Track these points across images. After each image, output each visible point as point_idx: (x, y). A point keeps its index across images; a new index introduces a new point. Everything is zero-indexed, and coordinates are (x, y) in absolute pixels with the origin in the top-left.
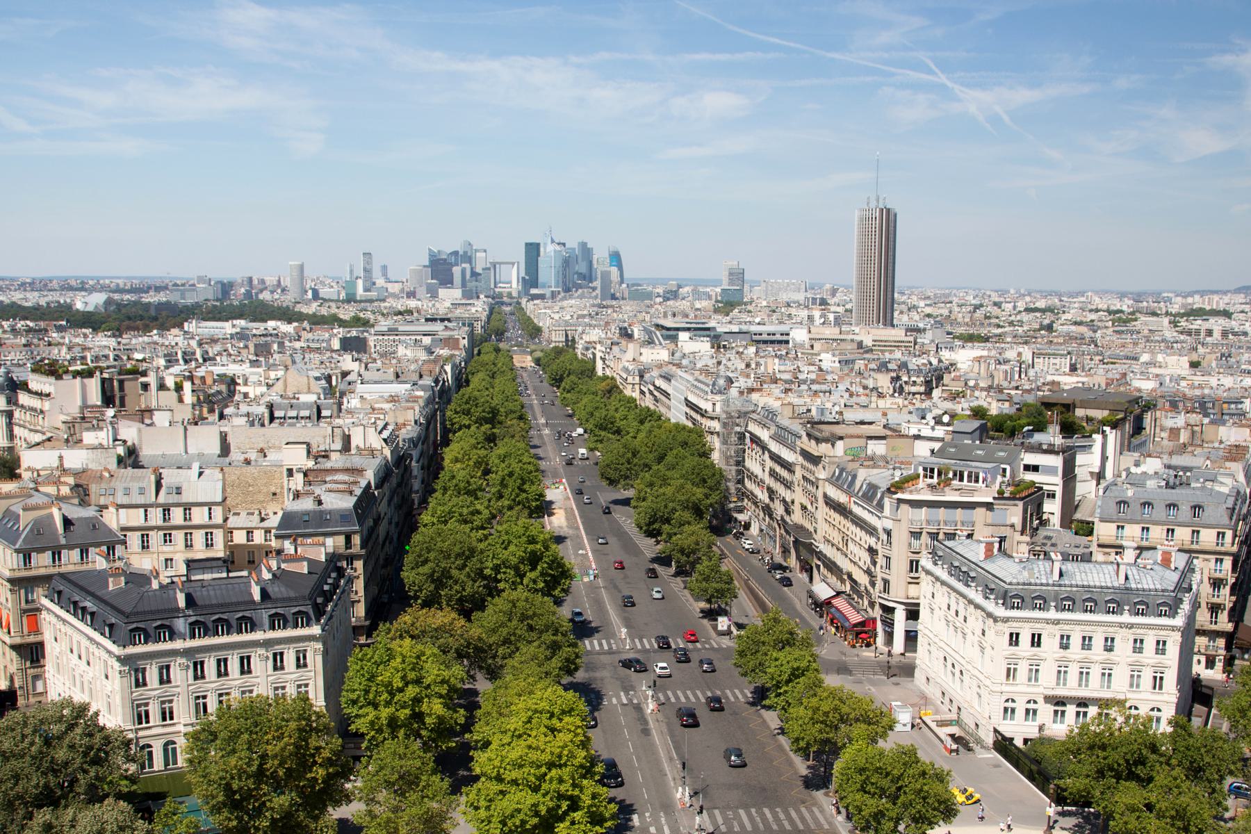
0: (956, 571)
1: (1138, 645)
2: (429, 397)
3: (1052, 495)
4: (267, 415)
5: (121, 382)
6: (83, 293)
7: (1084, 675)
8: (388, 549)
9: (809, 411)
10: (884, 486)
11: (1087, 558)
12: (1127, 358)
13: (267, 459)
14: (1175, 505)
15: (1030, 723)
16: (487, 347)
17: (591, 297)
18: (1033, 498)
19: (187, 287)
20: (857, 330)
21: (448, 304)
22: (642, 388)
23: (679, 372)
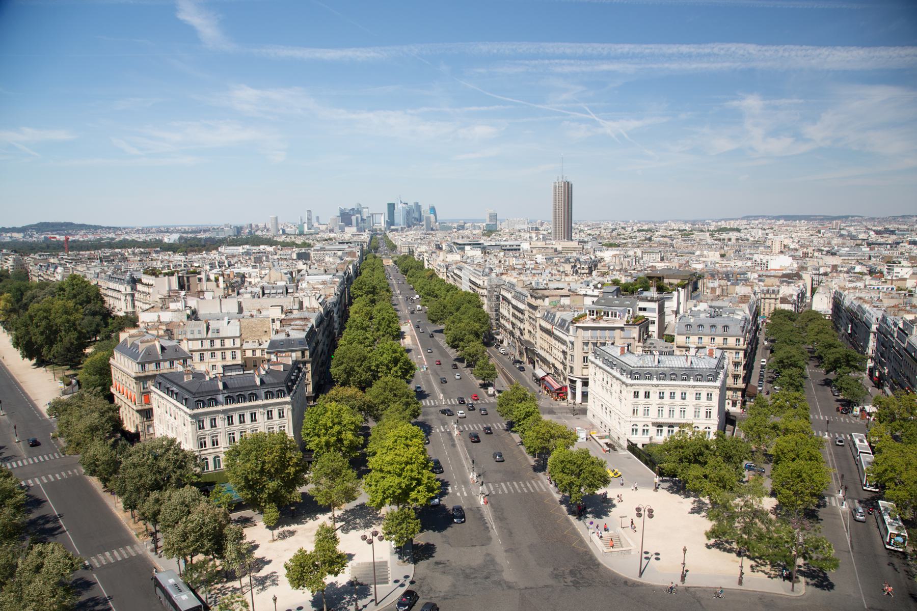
0: (608, 362)
1: (698, 396)
3: (653, 323)
4: (261, 293)
5: (188, 278)
7: (671, 412)
8: (323, 357)
9: (531, 283)
10: (569, 320)
11: (671, 353)
12: (689, 253)
14: (714, 326)
15: (645, 436)
16: (370, 256)
18: (644, 324)
20: (554, 242)
21: (350, 235)
23: (466, 266)
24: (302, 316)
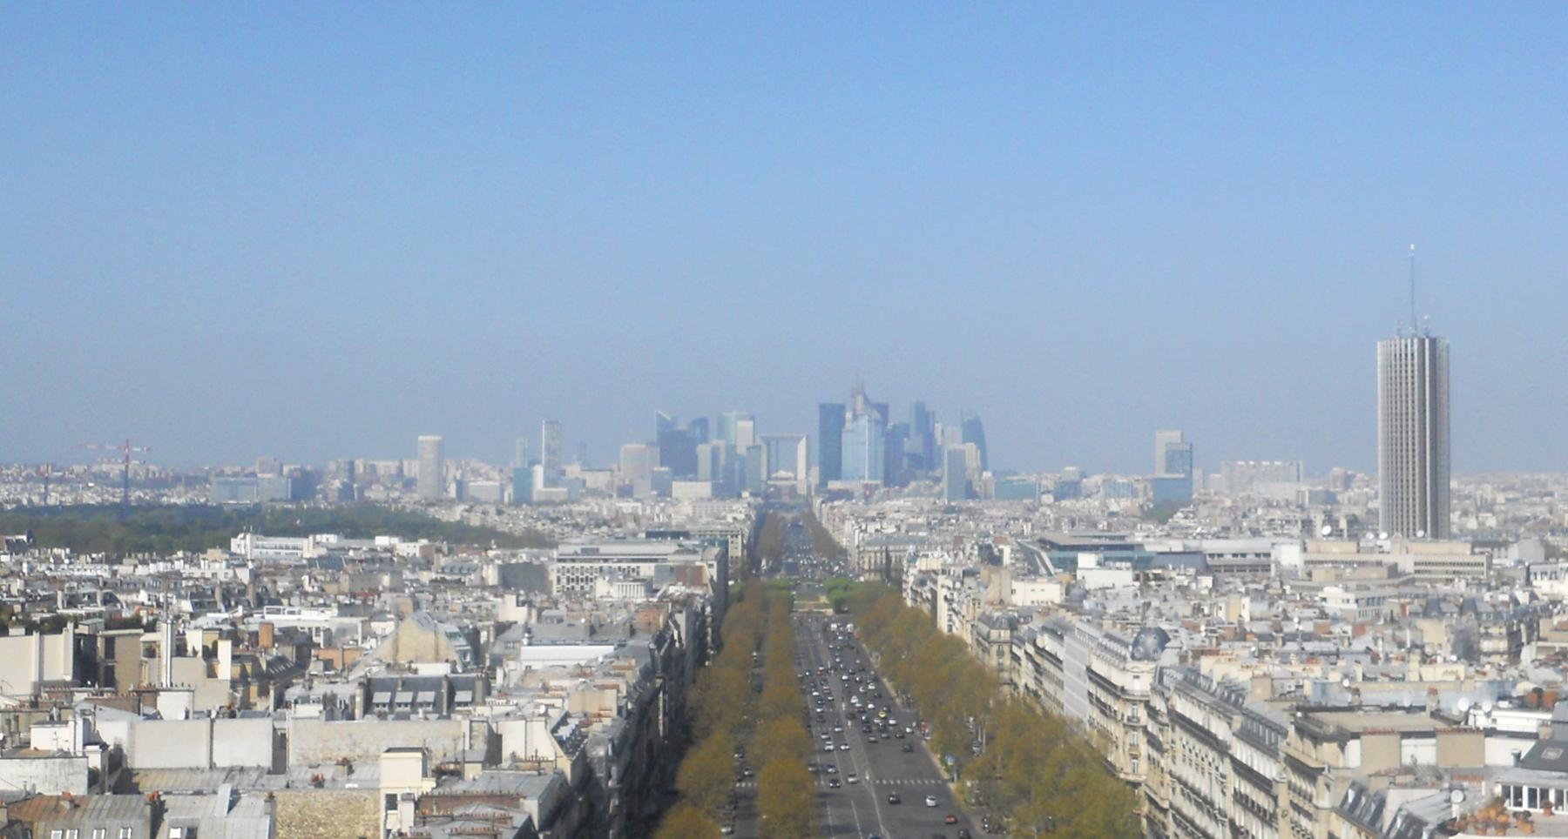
5: (110, 642)
13: (354, 776)
17: (931, 495)
20: (1387, 545)
22: (1015, 649)
24: (494, 787)
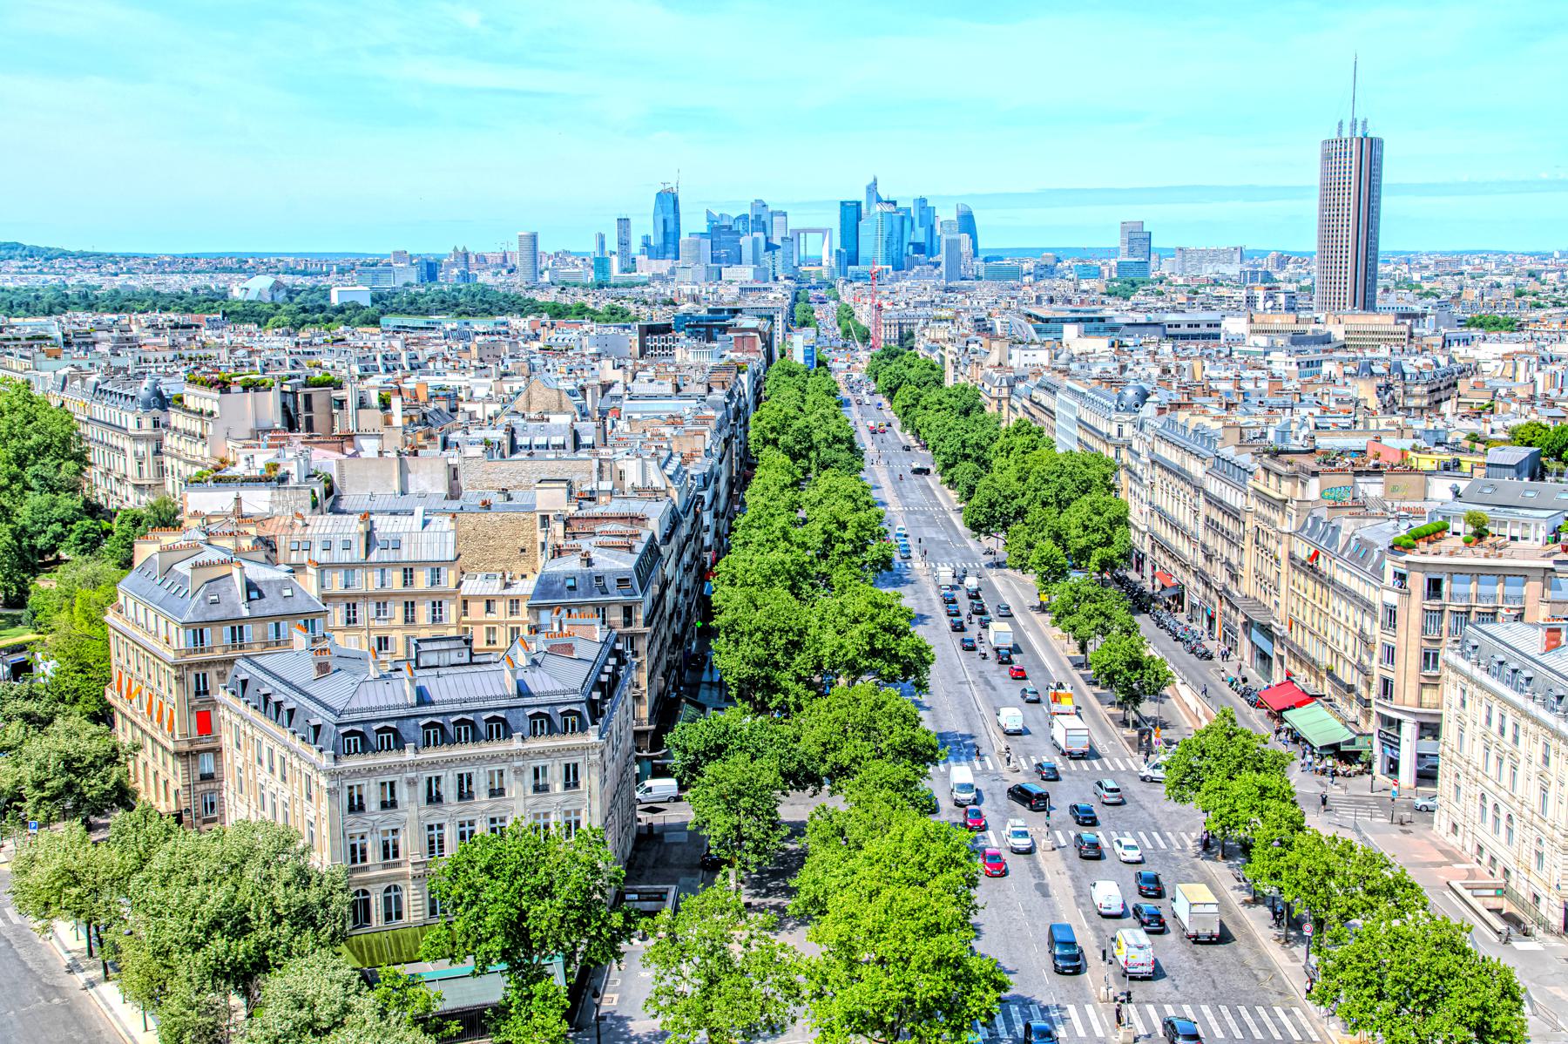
2: (722, 417)
6: (242, 276)
19: (380, 267)
